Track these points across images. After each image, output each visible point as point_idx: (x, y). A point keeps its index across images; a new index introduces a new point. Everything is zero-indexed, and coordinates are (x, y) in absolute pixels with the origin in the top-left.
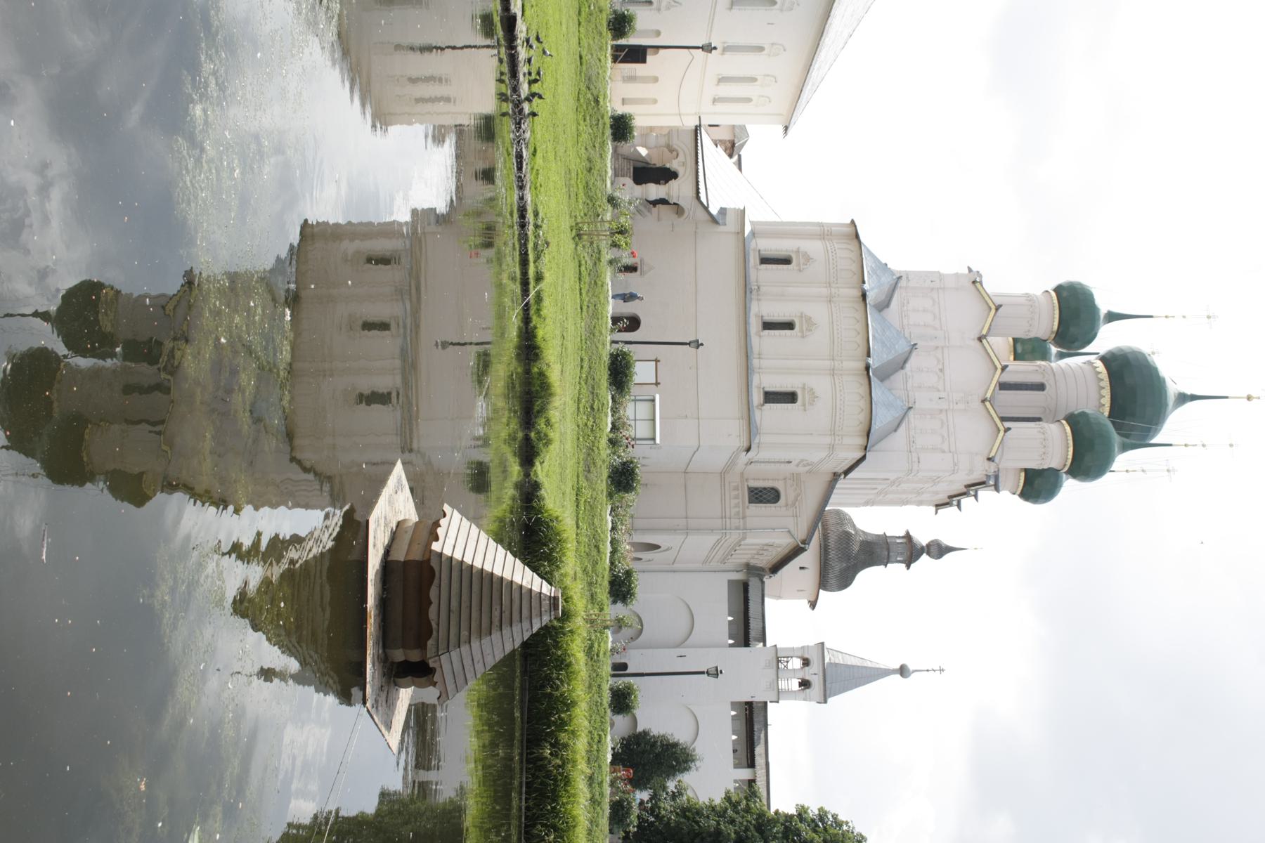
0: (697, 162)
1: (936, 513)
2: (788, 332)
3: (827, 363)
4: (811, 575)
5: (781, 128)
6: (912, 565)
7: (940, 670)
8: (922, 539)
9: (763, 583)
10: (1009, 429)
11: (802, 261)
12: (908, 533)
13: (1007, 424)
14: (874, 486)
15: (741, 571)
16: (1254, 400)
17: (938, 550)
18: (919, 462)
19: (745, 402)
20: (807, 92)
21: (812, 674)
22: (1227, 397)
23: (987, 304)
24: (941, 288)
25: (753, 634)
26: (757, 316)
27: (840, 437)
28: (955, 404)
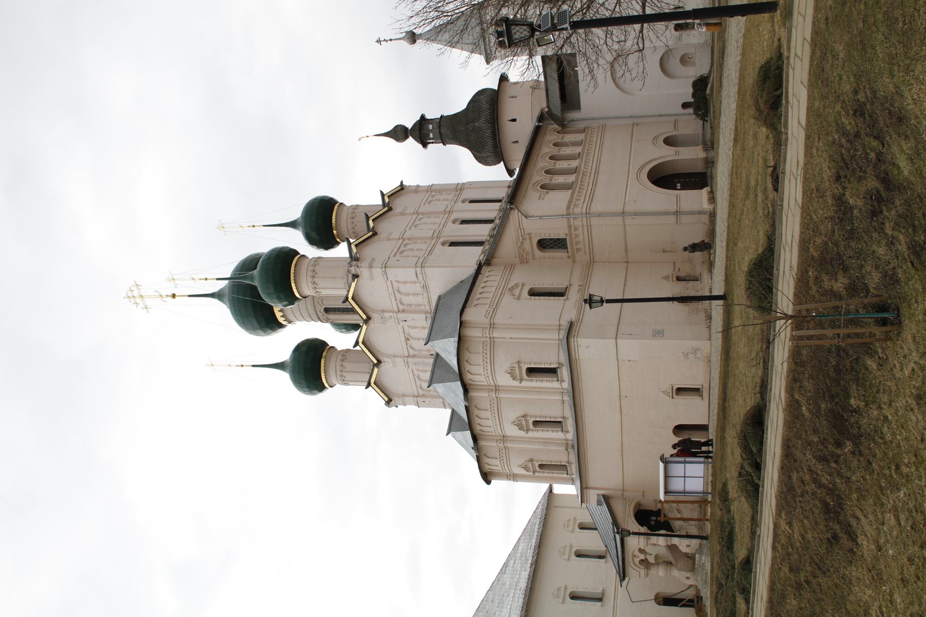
1: (402, 182)
2: (538, 419)
3: (501, 395)
7: (380, 41)
9: (548, 107)
11: (530, 465)
13: (346, 305)
15: (569, 122)
16: (170, 294)
18: (416, 274)
19: (575, 372)
20: (536, 530)
22: (190, 296)
24: (416, 397)
25: (554, 66)
27: (485, 335)
28: (392, 316)
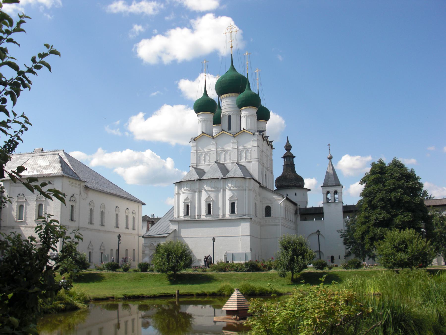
0: (155, 237)
1: (275, 149)
2: (211, 206)
4: (298, 191)
5: (143, 206)
6: (294, 156)
7: (329, 145)
8: (284, 152)
10: (243, 128)
12: (283, 157)
13: (242, 129)
14: (265, 172)
17: (288, 147)
21: (332, 190)
23: (202, 136)
26: (206, 216)
